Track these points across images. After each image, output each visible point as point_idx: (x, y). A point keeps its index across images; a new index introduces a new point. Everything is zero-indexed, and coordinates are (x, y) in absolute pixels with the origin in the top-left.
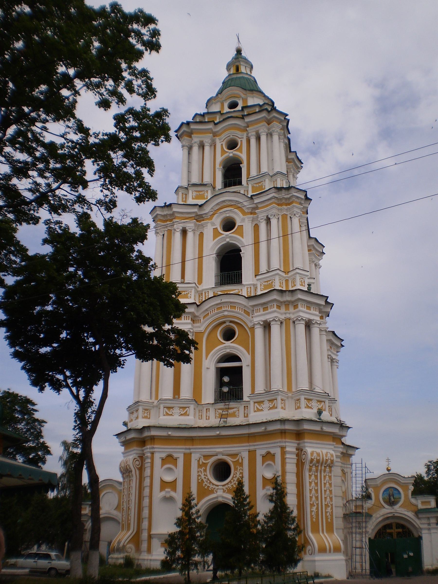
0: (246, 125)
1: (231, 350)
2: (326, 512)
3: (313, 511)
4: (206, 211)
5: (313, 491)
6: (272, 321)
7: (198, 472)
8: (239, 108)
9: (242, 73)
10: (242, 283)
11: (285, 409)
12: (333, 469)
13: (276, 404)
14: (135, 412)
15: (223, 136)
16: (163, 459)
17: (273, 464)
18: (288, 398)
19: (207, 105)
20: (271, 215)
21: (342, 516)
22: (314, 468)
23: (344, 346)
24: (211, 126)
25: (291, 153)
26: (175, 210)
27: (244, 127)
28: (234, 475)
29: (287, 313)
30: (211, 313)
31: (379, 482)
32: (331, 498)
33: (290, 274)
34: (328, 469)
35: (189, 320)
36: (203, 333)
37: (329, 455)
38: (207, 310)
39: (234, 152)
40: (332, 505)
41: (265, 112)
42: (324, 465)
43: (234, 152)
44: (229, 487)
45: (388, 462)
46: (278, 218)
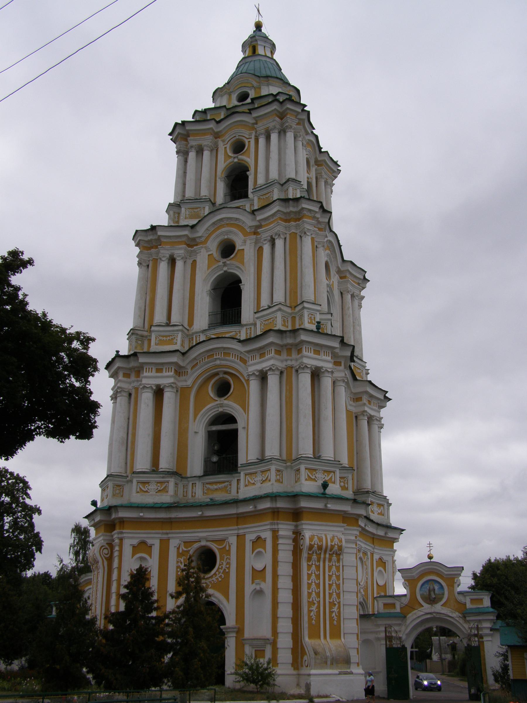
0: (254, 121)
1: (224, 408)
2: (331, 612)
3: (312, 611)
4: (199, 234)
5: (313, 586)
6: (269, 370)
7: (178, 562)
8: (249, 100)
9: (259, 55)
10: (240, 323)
11: (282, 482)
12: (341, 557)
13: (269, 476)
14: (106, 489)
15: (227, 137)
16: (134, 547)
17: (264, 551)
18: (286, 467)
19: (213, 99)
20: (275, 236)
21: (356, 616)
22: (315, 557)
23: (390, 399)
24: (211, 125)
25: (322, 155)
26: (160, 233)
27: (254, 124)
28: (219, 566)
29: (288, 359)
30: (200, 363)
31: (415, 574)
32: (338, 595)
33: (298, 309)
34: (334, 558)
35: (171, 372)
36: (192, 387)
37: (336, 539)
38: (195, 359)
40: (339, 603)
41: (276, 103)
42: (328, 552)
43: (240, 157)
44: (213, 580)
45: (430, 547)
46: (285, 238)
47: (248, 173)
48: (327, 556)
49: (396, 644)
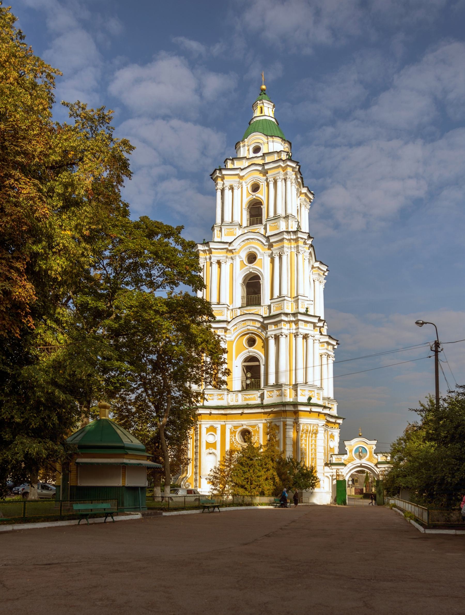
8: (260, 154)
10: (260, 304)
12: (317, 435)
34: (314, 436)
39: (256, 195)
42: (311, 433)
47: (262, 206)
48: (311, 435)
49: (341, 479)
